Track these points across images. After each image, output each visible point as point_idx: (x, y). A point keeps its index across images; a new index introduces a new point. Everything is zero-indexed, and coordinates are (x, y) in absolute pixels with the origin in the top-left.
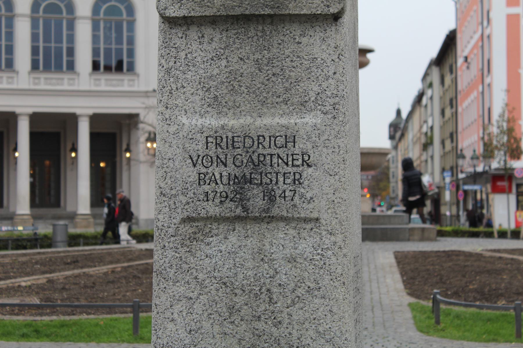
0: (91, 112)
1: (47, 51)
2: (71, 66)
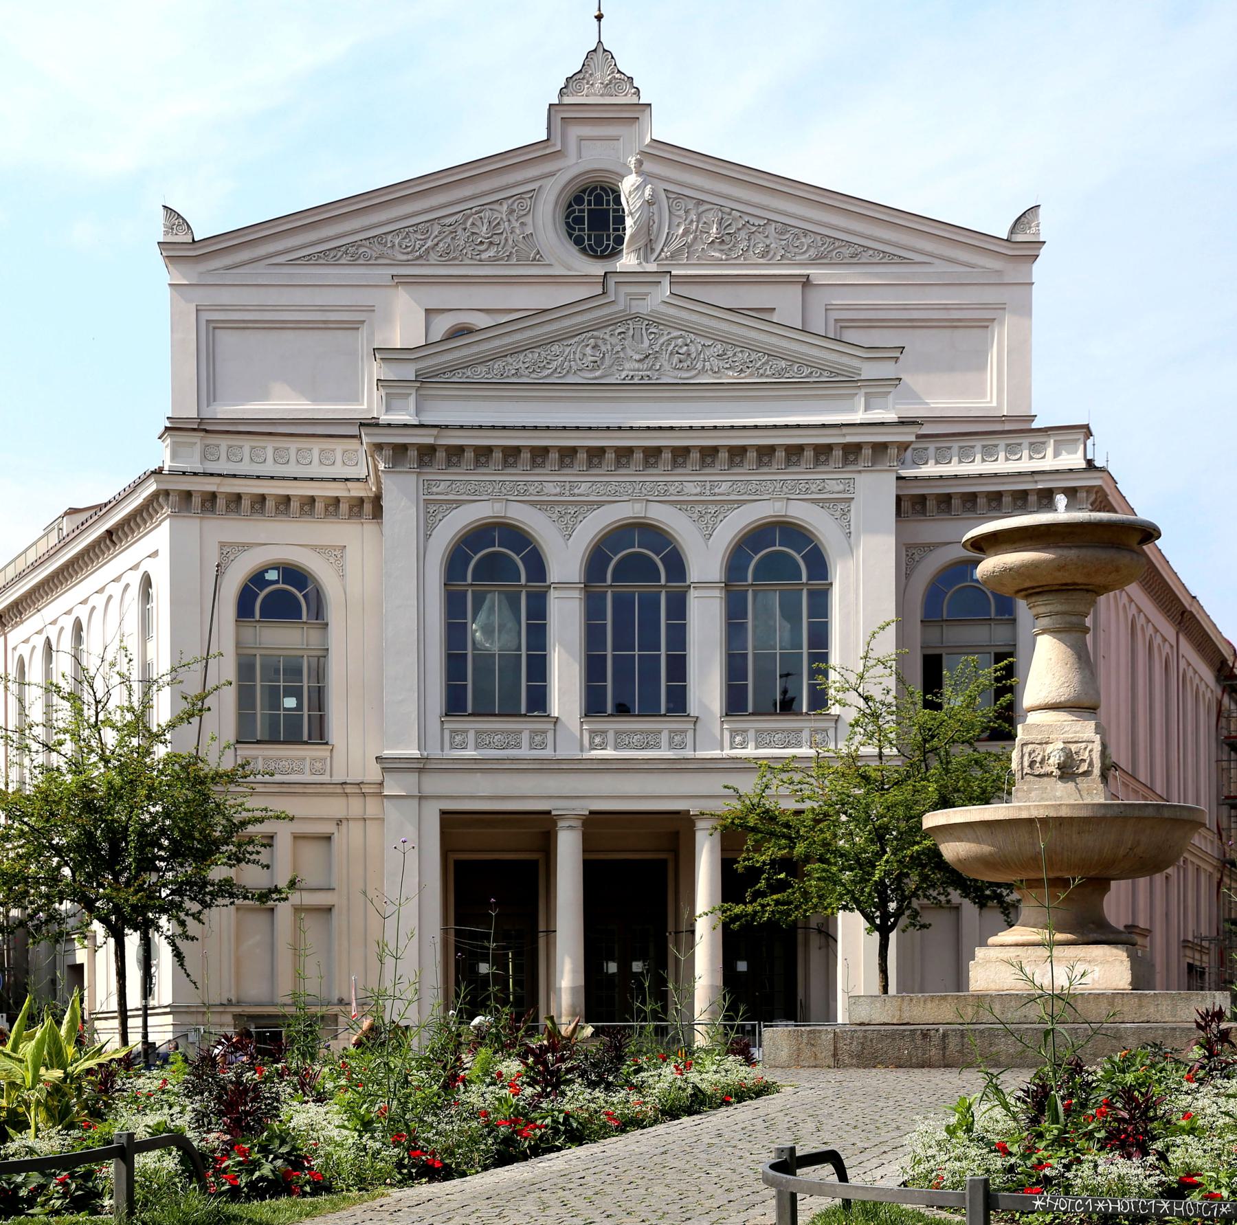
2: (678, 702)
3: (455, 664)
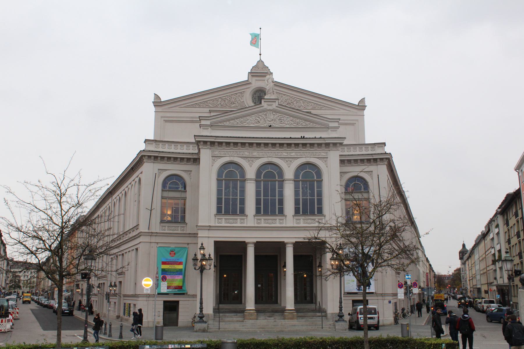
0: (294, 241)
1: (266, 201)
3: (219, 201)
